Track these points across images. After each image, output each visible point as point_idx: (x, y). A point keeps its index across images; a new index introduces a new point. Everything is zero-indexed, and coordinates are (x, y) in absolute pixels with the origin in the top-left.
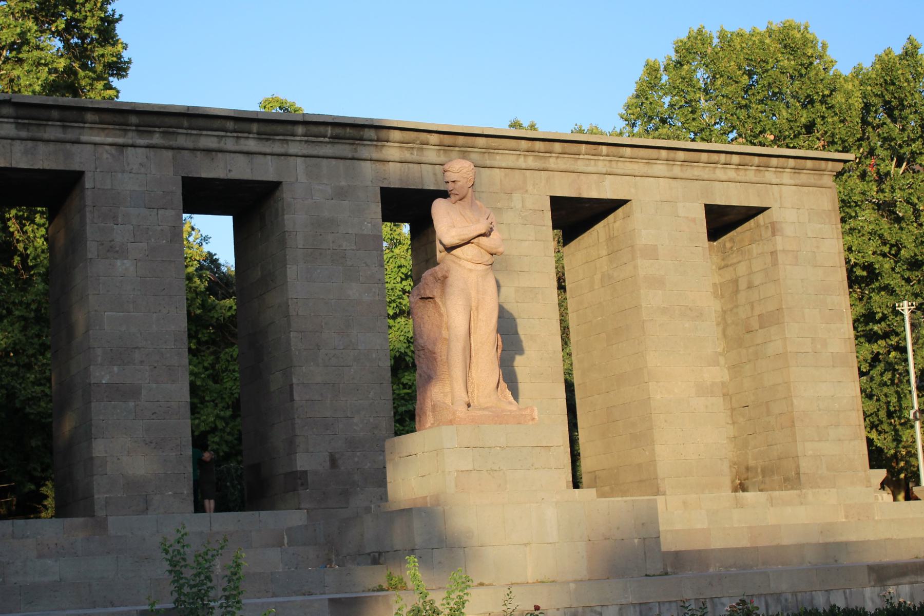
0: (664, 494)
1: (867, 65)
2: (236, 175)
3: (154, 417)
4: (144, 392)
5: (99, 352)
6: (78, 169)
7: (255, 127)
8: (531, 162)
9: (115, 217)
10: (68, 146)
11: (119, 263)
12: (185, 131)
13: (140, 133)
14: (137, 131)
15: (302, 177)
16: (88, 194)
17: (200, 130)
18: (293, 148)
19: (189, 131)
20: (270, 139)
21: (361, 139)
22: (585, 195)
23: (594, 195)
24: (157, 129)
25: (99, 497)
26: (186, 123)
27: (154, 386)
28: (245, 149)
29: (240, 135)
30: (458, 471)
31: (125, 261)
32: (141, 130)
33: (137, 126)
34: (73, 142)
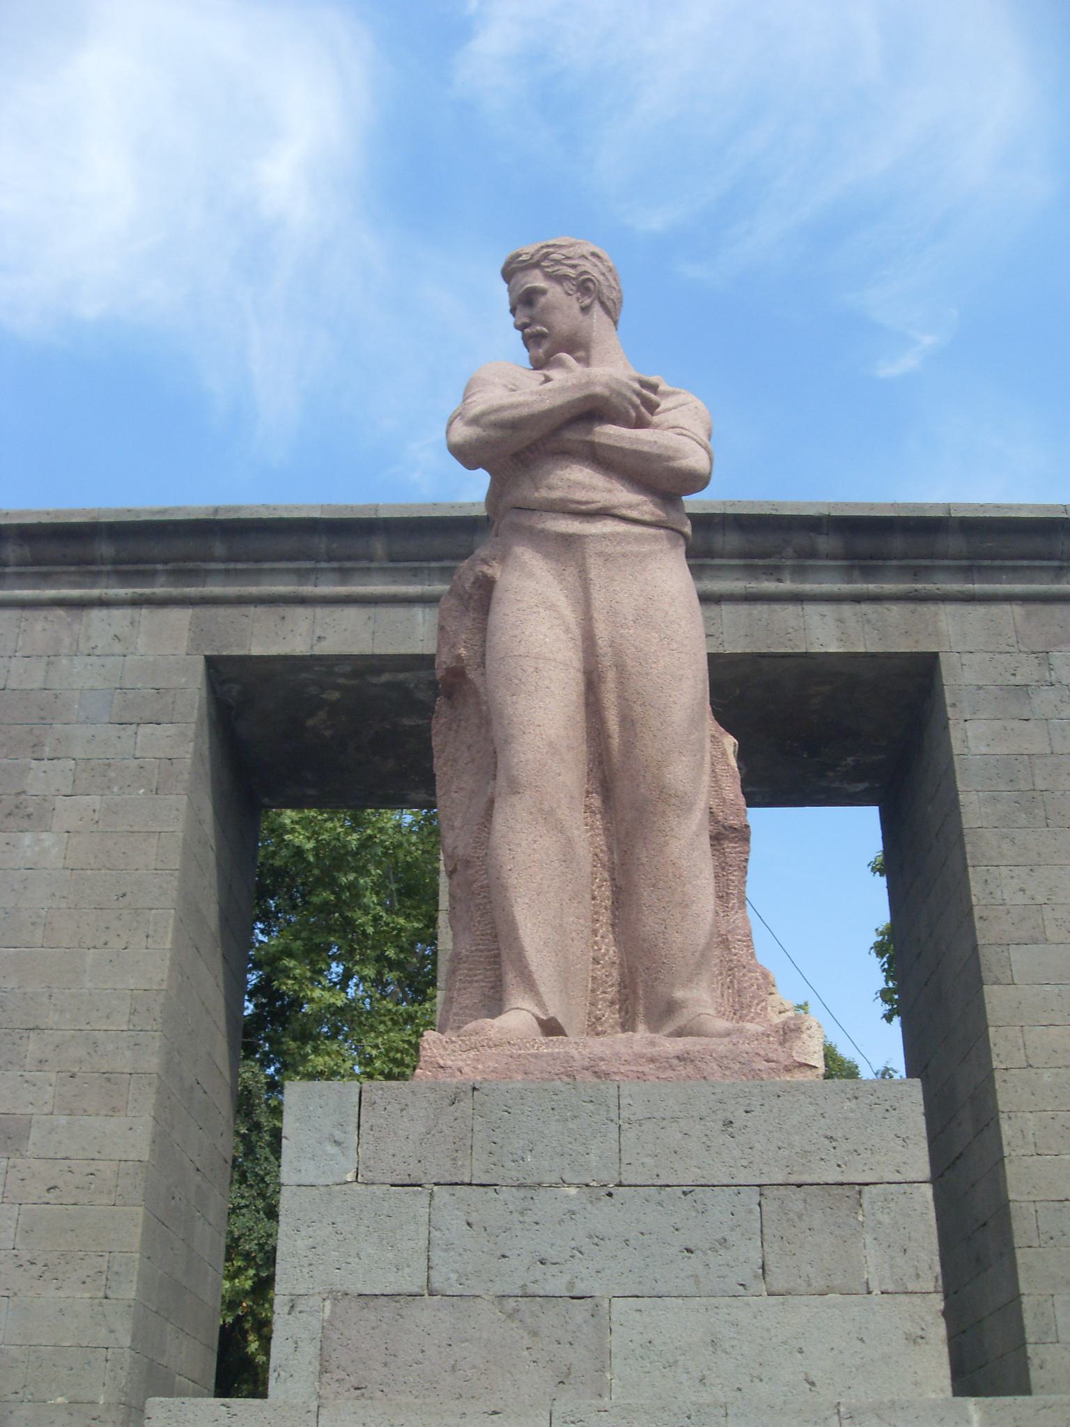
2: (330, 647)
3: (50, 1197)
4: (35, 1134)
7: (378, 546)
9: (37, 745)
11: (27, 839)
12: (221, 566)
13: (125, 577)
14: (118, 573)
17: (257, 561)
19: (232, 566)
20: (421, 570)
24: (159, 567)
26: (219, 548)
27: (63, 1120)
29: (348, 564)
30: (338, 1296)
31: (44, 836)
33: (115, 562)
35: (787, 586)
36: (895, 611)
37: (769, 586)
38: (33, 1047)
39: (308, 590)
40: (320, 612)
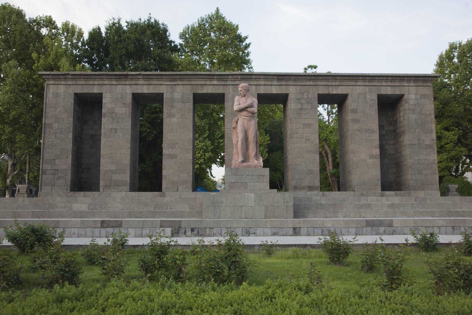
0: (354, 191)
1: (464, 42)
2: (210, 91)
5: (165, 145)
6: (162, 92)
7: (215, 77)
8: (311, 83)
10: (159, 86)
15: (231, 91)
16: (164, 99)
18: (228, 83)
21: (251, 79)
22: (331, 93)
23: (334, 92)
25: (164, 186)
28: (213, 83)
32: (180, 79)
34: (161, 85)
35: (270, 83)
36: (284, 87)
37: (267, 83)
38: (177, 146)
39: (206, 83)
40: (208, 86)
